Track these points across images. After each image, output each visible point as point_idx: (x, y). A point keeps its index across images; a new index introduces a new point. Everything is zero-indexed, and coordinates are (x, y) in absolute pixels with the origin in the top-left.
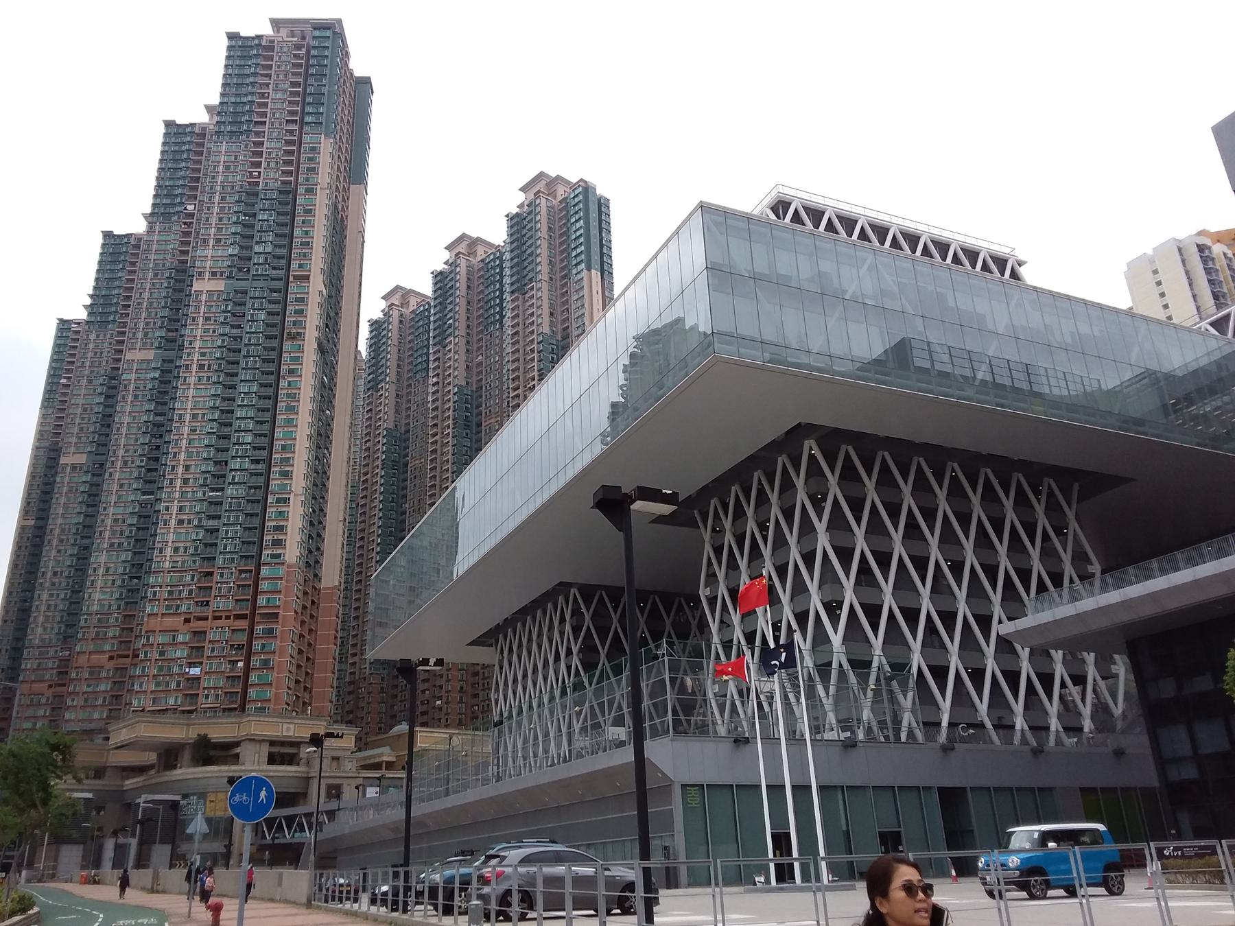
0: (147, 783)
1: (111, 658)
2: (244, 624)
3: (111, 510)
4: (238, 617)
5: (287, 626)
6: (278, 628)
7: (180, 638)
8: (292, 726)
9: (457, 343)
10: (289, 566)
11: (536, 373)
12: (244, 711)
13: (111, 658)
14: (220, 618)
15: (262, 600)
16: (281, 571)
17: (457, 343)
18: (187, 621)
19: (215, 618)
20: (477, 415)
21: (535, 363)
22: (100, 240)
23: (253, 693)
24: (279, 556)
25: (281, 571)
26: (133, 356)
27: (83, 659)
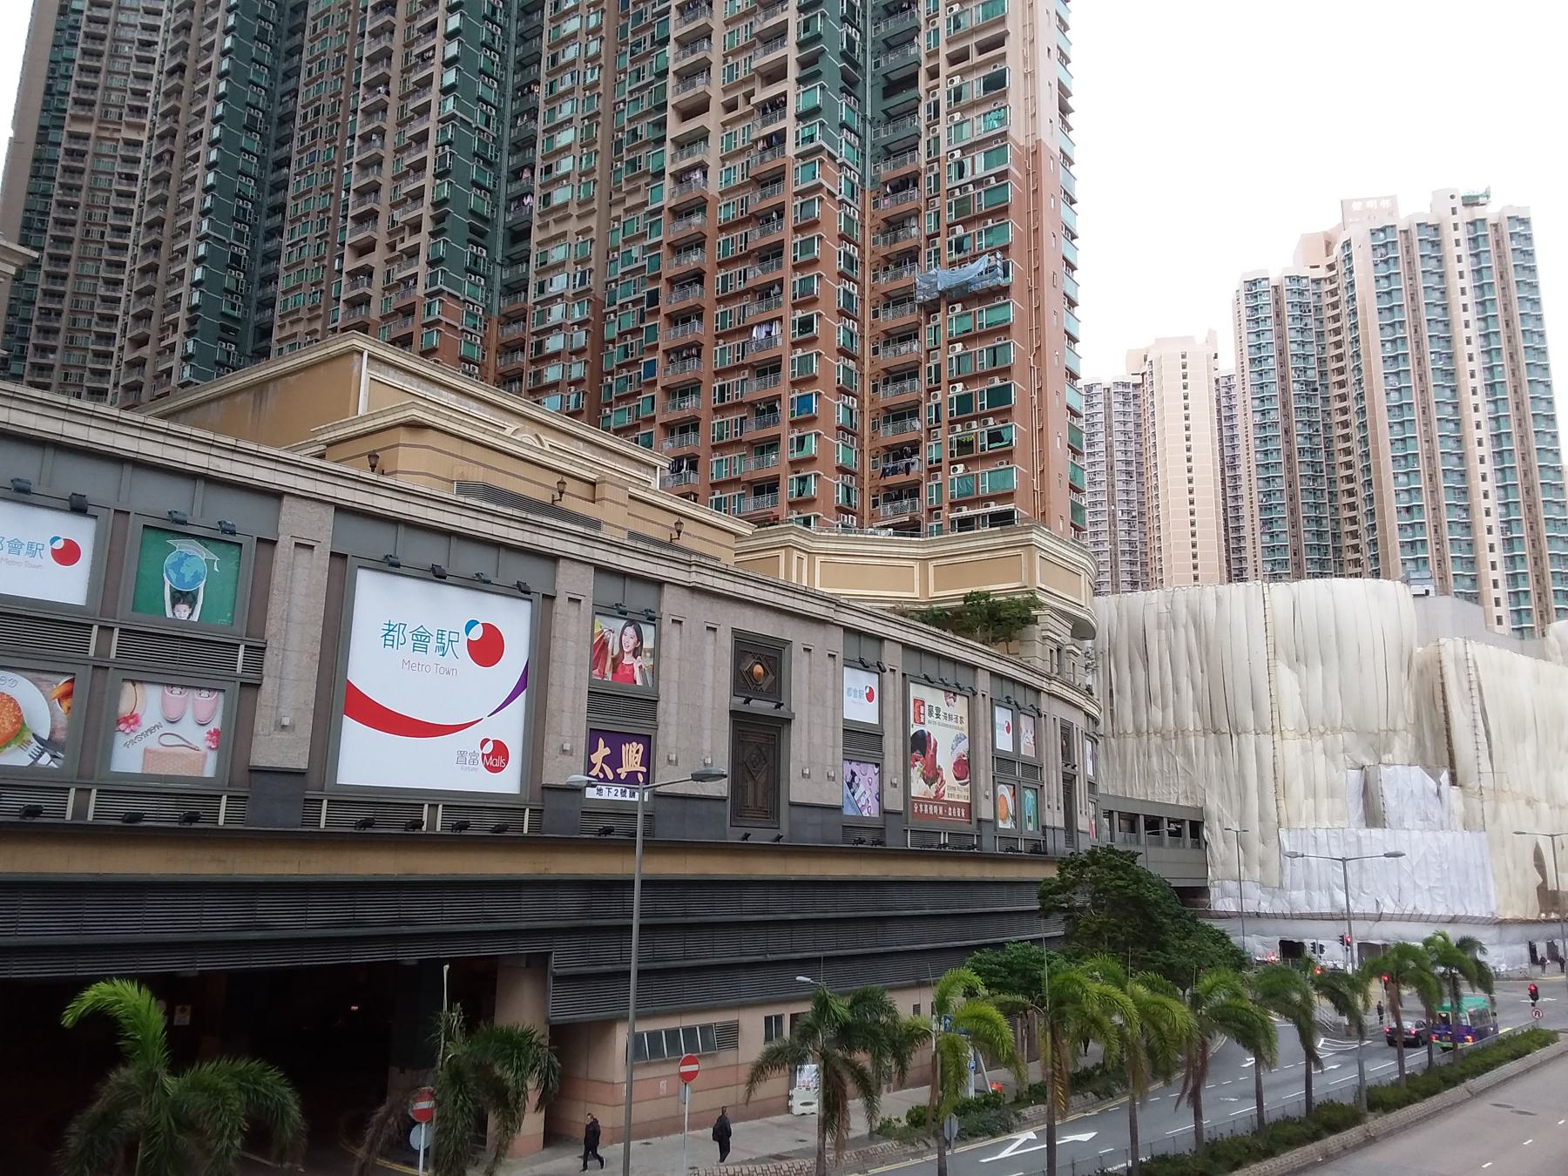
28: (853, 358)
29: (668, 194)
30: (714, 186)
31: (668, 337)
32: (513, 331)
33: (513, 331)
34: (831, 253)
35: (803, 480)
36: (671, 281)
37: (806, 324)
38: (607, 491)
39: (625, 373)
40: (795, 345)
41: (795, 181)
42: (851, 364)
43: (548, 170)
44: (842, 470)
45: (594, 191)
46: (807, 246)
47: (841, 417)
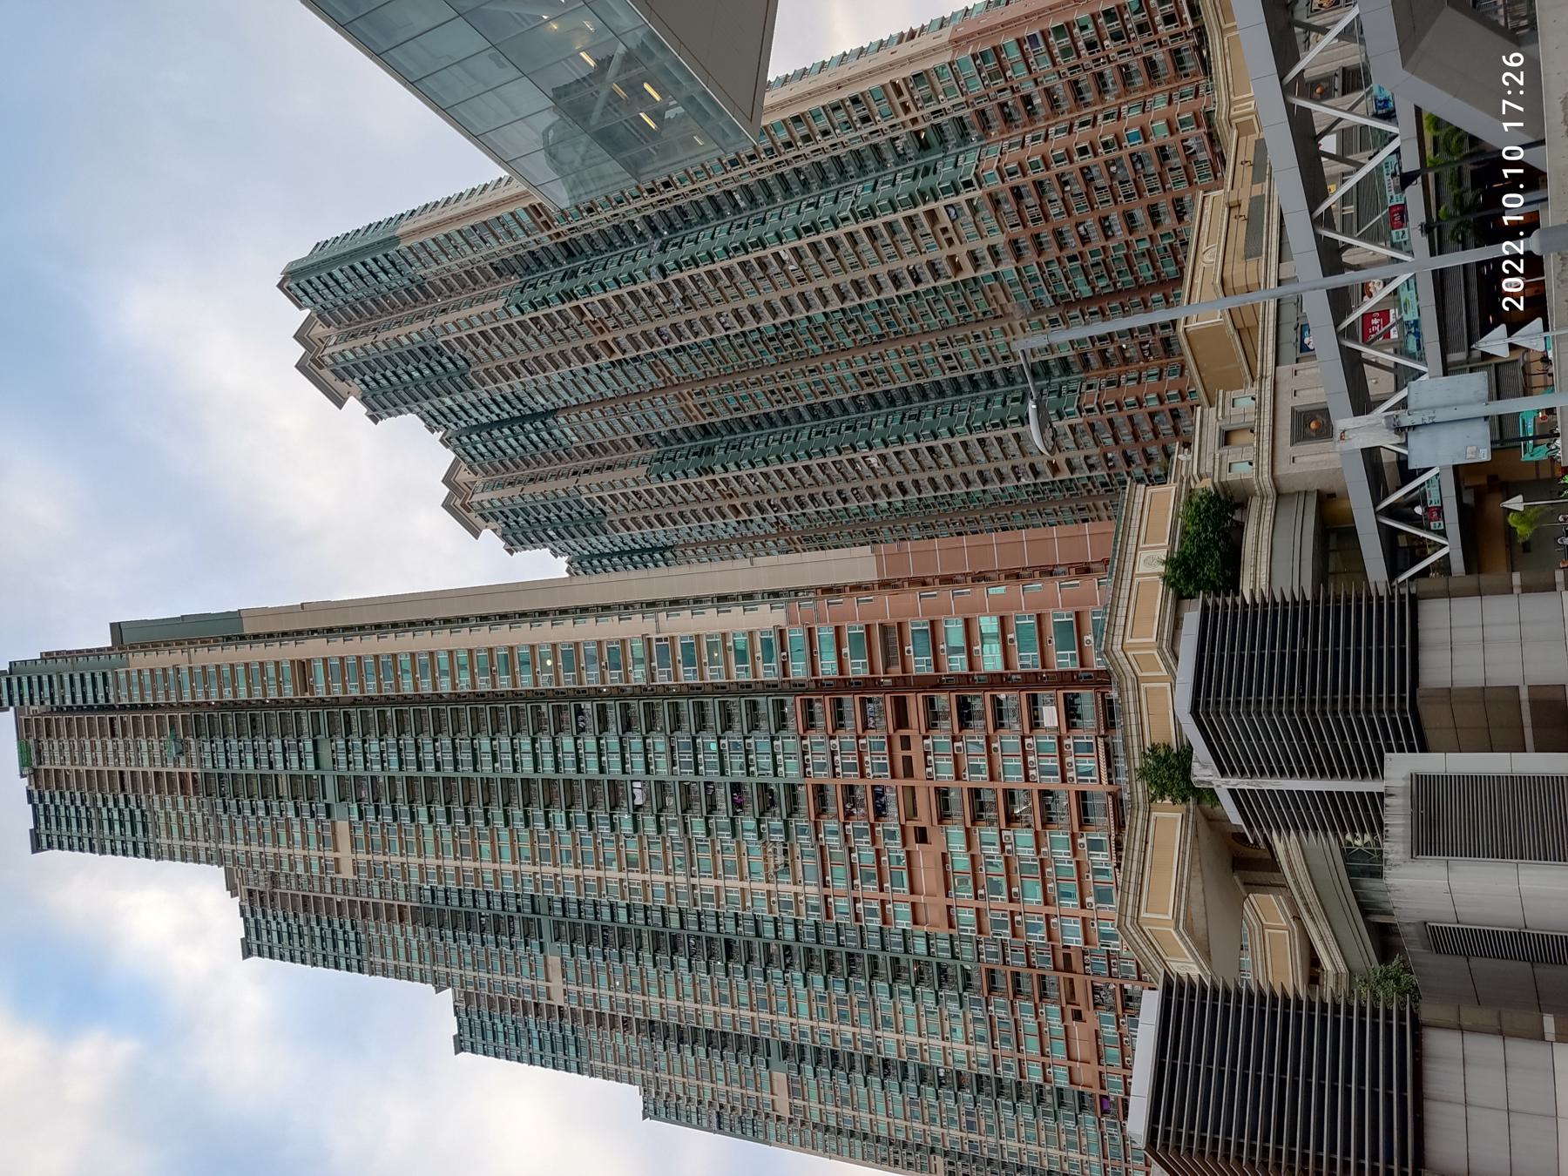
0: (1316, 908)
1: (1078, 1016)
2: (915, 704)
3: (805, 1023)
4: (902, 721)
5: (910, 608)
6: (916, 624)
7: (958, 845)
8: (1143, 555)
9: (591, 487)
10: (791, 621)
11: (567, 306)
12: (1107, 673)
13: (1078, 1016)
14: (908, 761)
15: (857, 669)
16: (796, 634)
17: (591, 487)
18: (922, 836)
19: (909, 773)
20: (692, 438)
21: (553, 310)
22: (466, 1056)
23: (1063, 661)
24: (767, 644)
25: (796, 634)
26: (557, 991)
27: (1086, 1074)
28: (1095, 118)
29: (1008, 266)
30: (999, 239)
31: (1097, 241)
32: (1094, 361)
33: (1094, 361)
34: (1033, 151)
35: (1183, 123)
36: (1061, 249)
37: (1083, 151)
38: (1233, 199)
39: (1114, 274)
40: (1096, 155)
41: (995, 185)
42: (1100, 117)
43: (987, 362)
44: (1170, 102)
45: (996, 329)
46: (1035, 165)
47: (1136, 113)
